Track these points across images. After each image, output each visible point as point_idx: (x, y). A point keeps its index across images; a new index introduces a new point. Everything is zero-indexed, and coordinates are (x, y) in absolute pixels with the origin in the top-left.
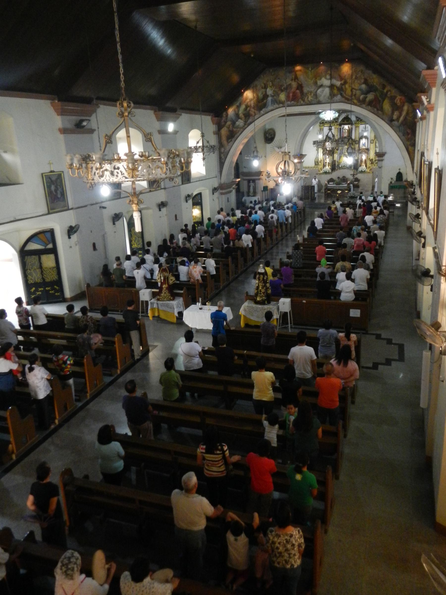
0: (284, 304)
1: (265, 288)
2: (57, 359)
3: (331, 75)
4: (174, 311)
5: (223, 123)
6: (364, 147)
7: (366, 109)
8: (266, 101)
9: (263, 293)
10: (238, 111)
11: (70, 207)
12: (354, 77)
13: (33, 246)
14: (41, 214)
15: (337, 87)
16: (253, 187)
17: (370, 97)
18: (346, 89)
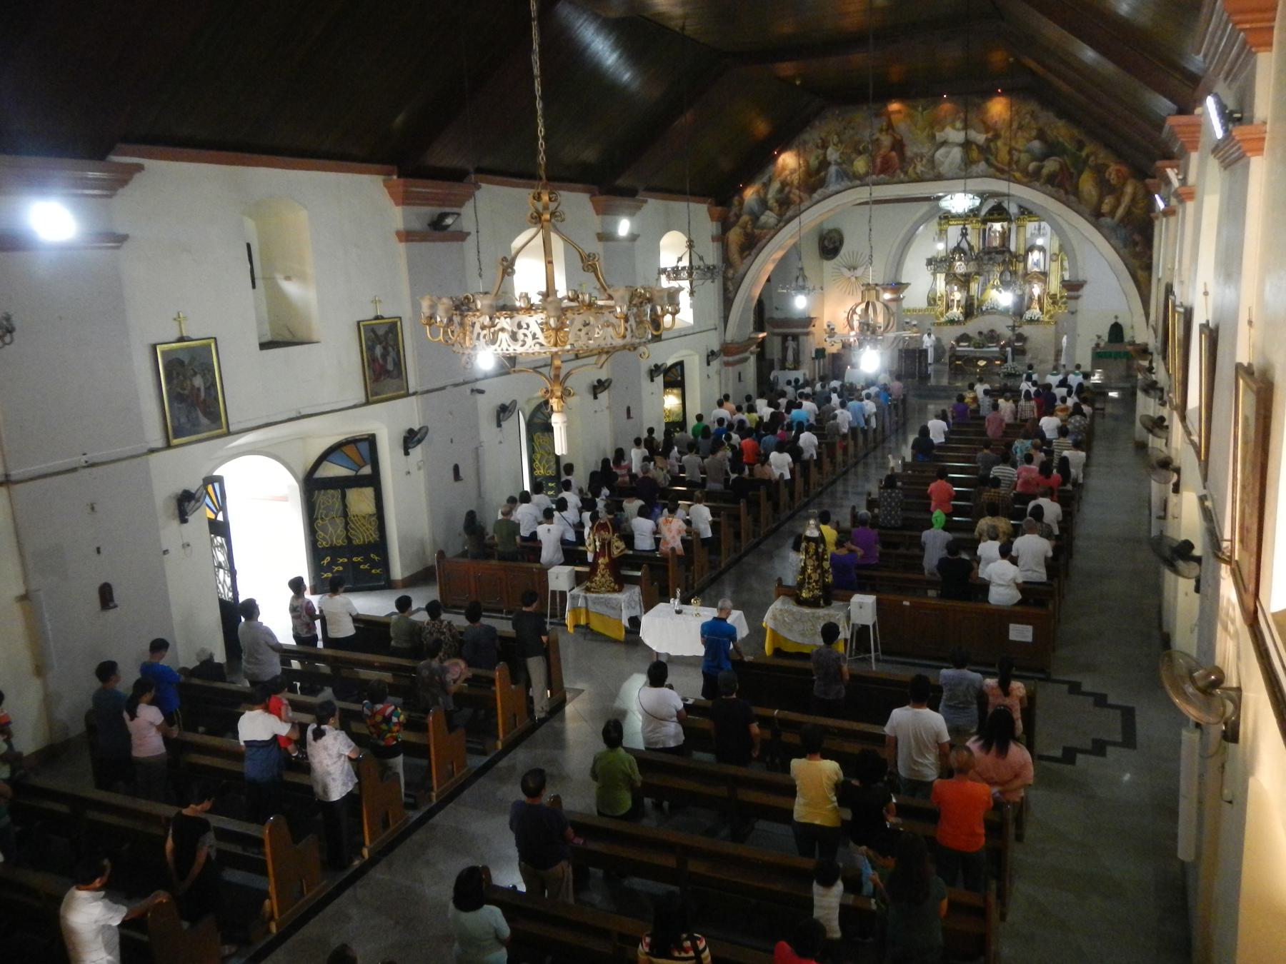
1: (819, 571)
2: (372, 711)
4: (621, 616)
5: (732, 219)
6: (1036, 269)
7: (1044, 192)
8: (826, 175)
9: (816, 582)
10: (766, 194)
11: (411, 391)
12: (1015, 126)
13: (332, 470)
14: (351, 404)
15: (978, 146)
16: (794, 349)
17: (1051, 165)
18: (997, 149)
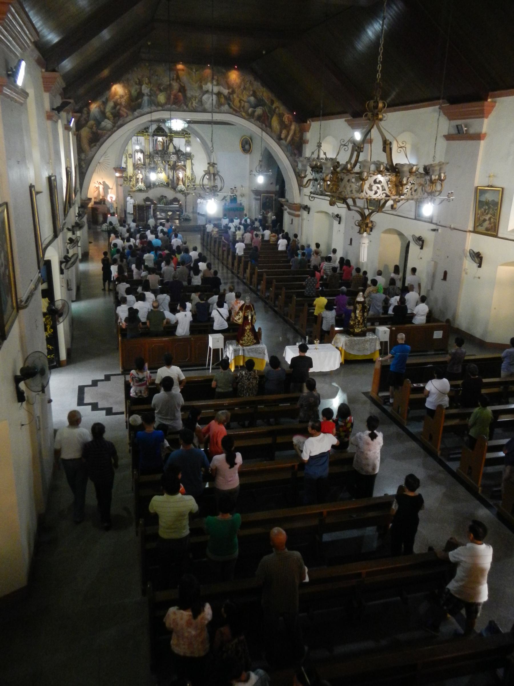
0: (385, 333)
3: (217, 80)
8: (142, 101)
10: (105, 108)
12: (242, 87)
15: (224, 96)
17: (259, 111)
18: (234, 98)
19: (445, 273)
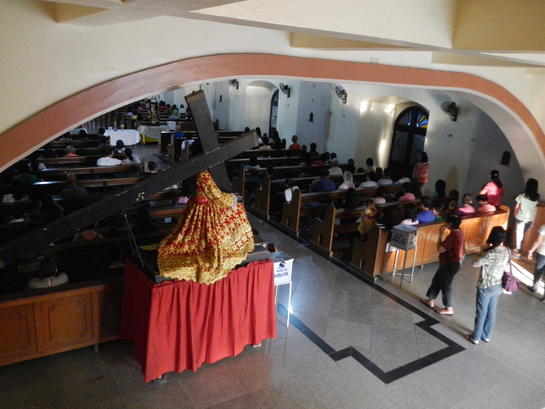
0: (173, 124)
9: (156, 118)
19: (221, 97)
